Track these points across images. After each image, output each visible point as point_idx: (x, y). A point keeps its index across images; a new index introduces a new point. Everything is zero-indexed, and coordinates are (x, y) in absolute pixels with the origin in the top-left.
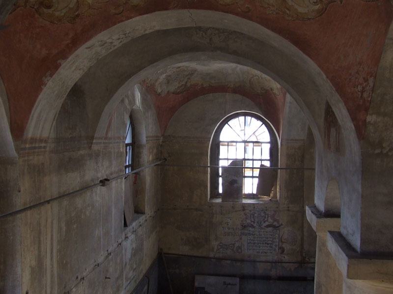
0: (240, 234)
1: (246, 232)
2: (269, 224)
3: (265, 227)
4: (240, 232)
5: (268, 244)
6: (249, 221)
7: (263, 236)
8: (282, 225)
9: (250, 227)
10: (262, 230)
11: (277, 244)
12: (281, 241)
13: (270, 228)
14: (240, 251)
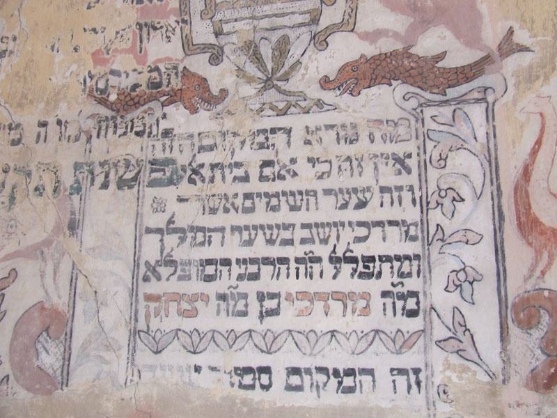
0: (68, 179)
1: (133, 148)
2: (370, 50)
3: (325, 83)
4: (67, 157)
5: (367, 267)
6: (162, 49)
7: (306, 178)
8: (509, 46)
9: (174, 97)
10: (296, 122)
11: (480, 257)
12: (529, 225)
13: (379, 93)
14: (50, 359)
